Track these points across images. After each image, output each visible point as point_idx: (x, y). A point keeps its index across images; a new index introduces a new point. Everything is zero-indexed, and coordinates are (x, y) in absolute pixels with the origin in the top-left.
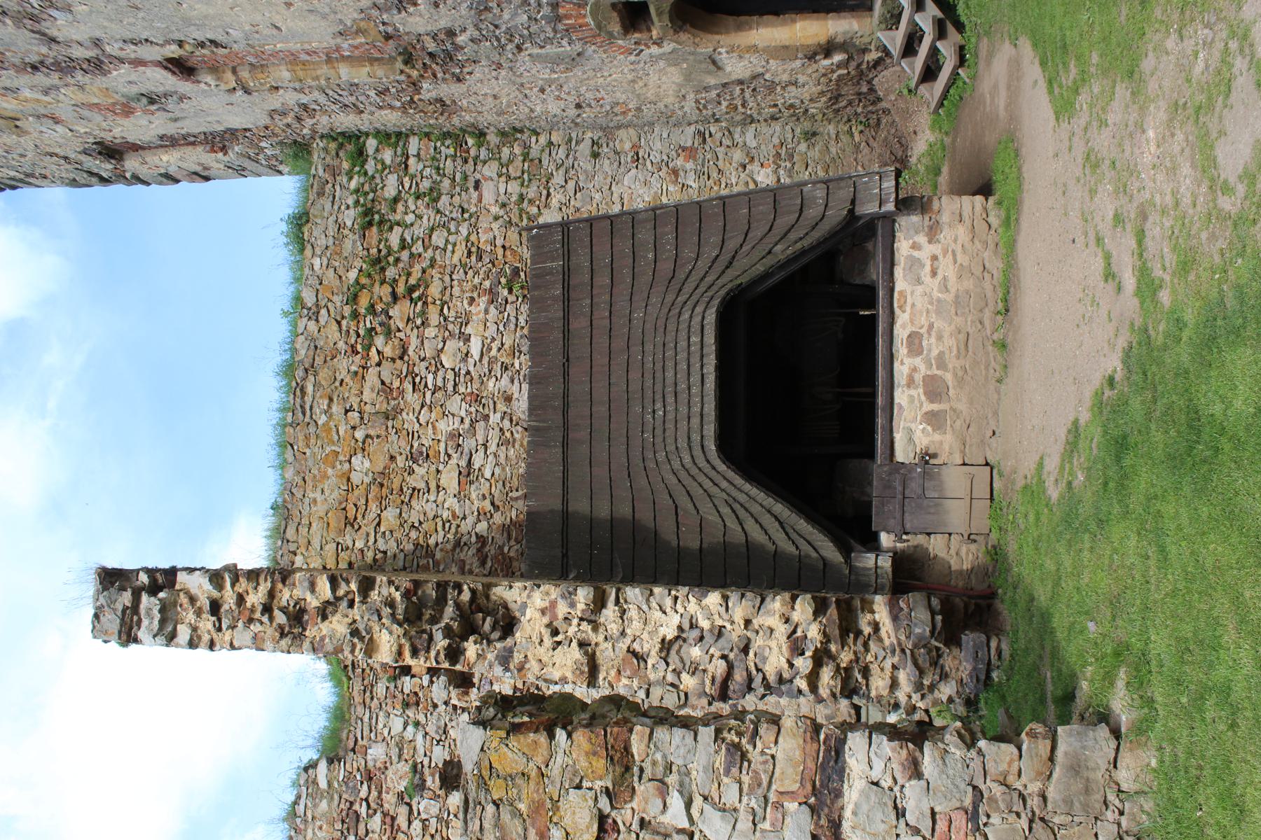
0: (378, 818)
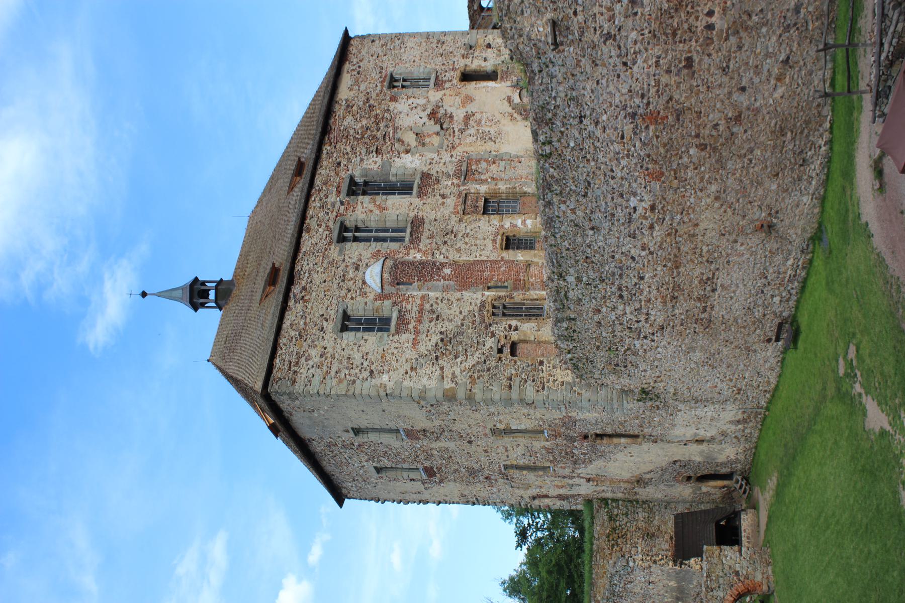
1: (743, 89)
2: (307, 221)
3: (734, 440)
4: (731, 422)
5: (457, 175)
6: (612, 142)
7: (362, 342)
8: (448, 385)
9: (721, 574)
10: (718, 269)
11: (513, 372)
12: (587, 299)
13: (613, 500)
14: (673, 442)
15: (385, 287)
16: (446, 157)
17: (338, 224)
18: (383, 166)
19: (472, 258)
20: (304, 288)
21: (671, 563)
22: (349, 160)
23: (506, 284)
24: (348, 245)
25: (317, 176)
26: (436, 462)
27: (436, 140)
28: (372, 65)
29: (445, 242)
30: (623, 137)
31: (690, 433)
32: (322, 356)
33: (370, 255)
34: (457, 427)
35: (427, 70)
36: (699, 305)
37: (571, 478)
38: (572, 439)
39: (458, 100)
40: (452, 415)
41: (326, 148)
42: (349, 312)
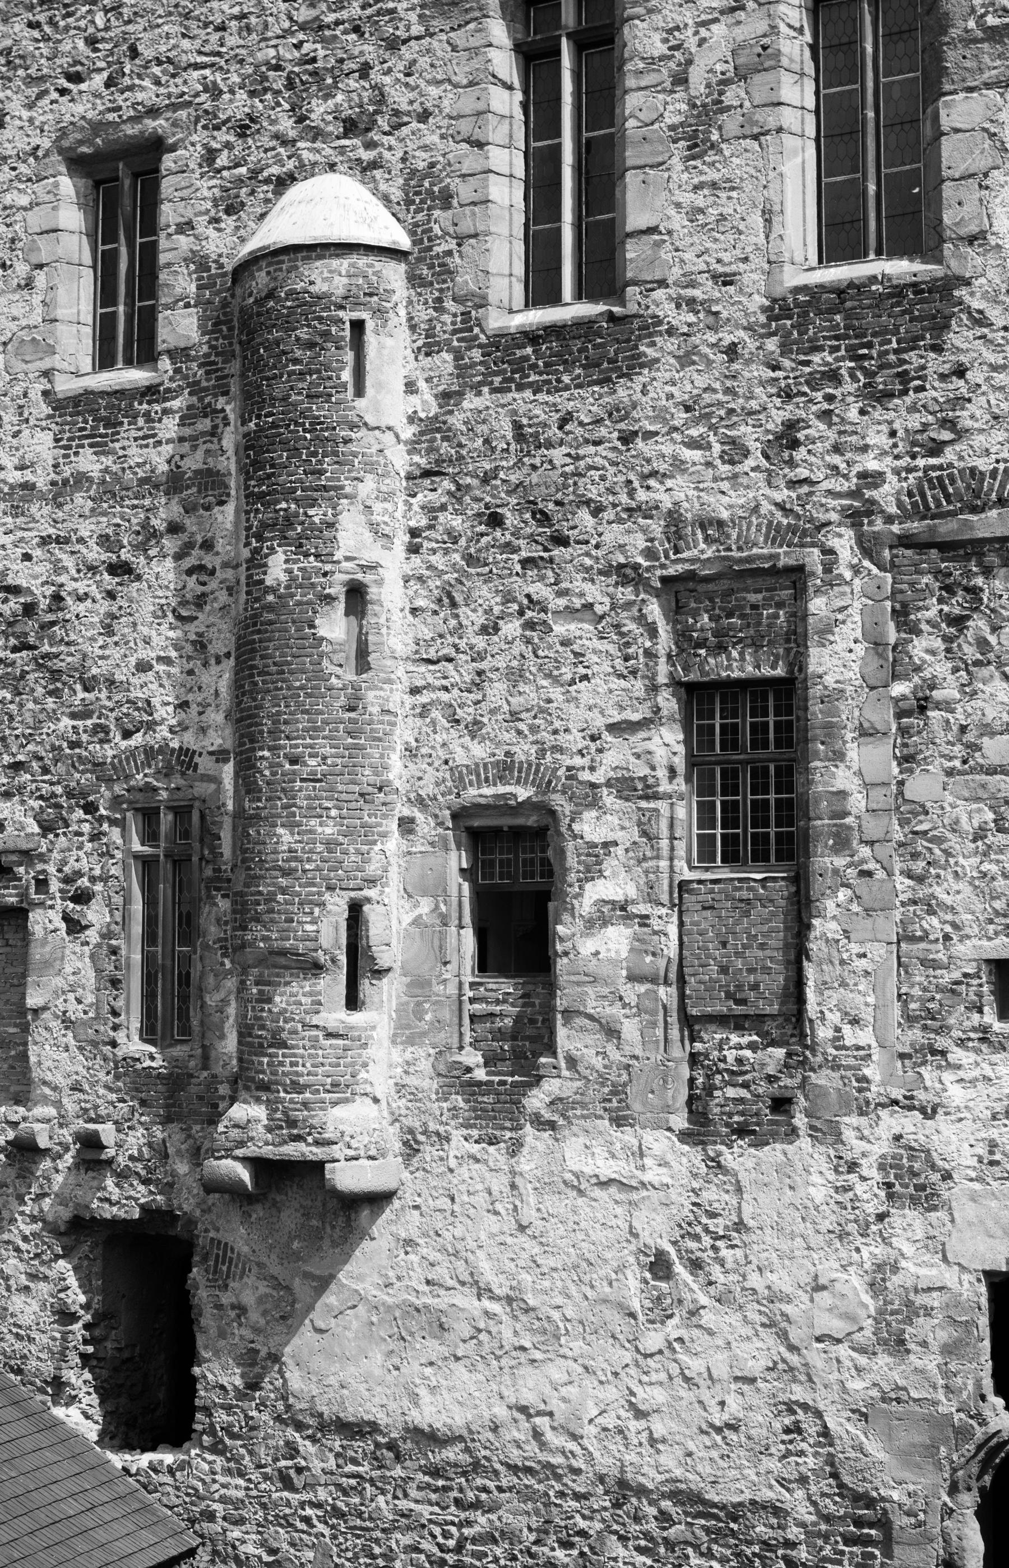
29: (495, 521)
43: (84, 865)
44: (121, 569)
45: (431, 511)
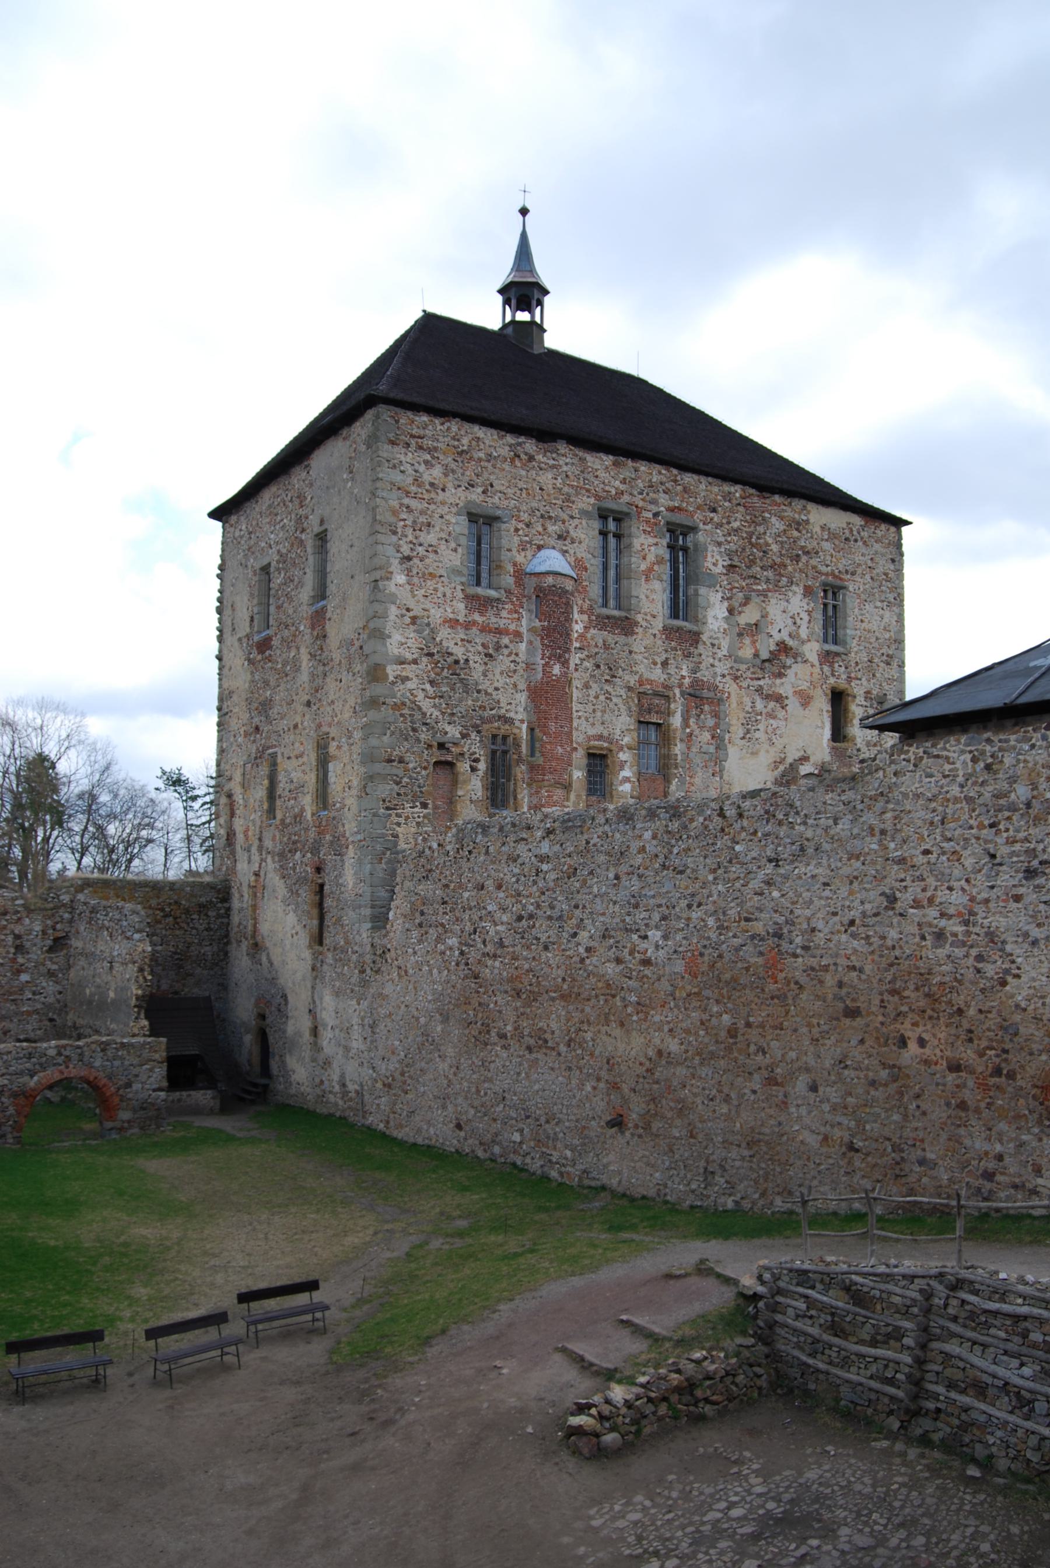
0: (5, 923)
1: (814, 1088)
2: (630, 463)
3: (317, 1080)
4: (343, 1076)
5: (696, 683)
6: (741, 904)
7: (453, 545)
8: (392, 671)
9: (127, 1063)
10: (559, 1054)
11: (411, 766)
12: (516, 871)
13: (229, 909)
14: (313, 993)
15: (534, 579)
16: (721, 668)
17: (625, 509)
18: (711, 575)
19: (575, 706)
20: (531, 458)
21: (140, 992)
22: (719, 525)
23: (538, 754)
24: (596, 525)
25: (696, 477)
26: (278, 652)
27: (747, 652)
28: (858, 558)
29: (598, 667)
30: (747, 920)
31: (327, 1016)
32: (432, 484)
33: (579, 556)
34: (331, 685)
35: (848, 639)
36: (509, 1028)
37: (260, 848)
38: (315, 850)
39: (804, 685)
40: (345, 677)
41: (737, 491)
42: (496, 525)
43: (477, 750)
44: (488, 655)
45: (582, 660)
